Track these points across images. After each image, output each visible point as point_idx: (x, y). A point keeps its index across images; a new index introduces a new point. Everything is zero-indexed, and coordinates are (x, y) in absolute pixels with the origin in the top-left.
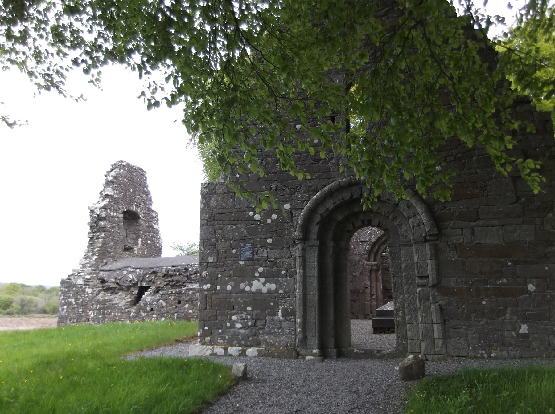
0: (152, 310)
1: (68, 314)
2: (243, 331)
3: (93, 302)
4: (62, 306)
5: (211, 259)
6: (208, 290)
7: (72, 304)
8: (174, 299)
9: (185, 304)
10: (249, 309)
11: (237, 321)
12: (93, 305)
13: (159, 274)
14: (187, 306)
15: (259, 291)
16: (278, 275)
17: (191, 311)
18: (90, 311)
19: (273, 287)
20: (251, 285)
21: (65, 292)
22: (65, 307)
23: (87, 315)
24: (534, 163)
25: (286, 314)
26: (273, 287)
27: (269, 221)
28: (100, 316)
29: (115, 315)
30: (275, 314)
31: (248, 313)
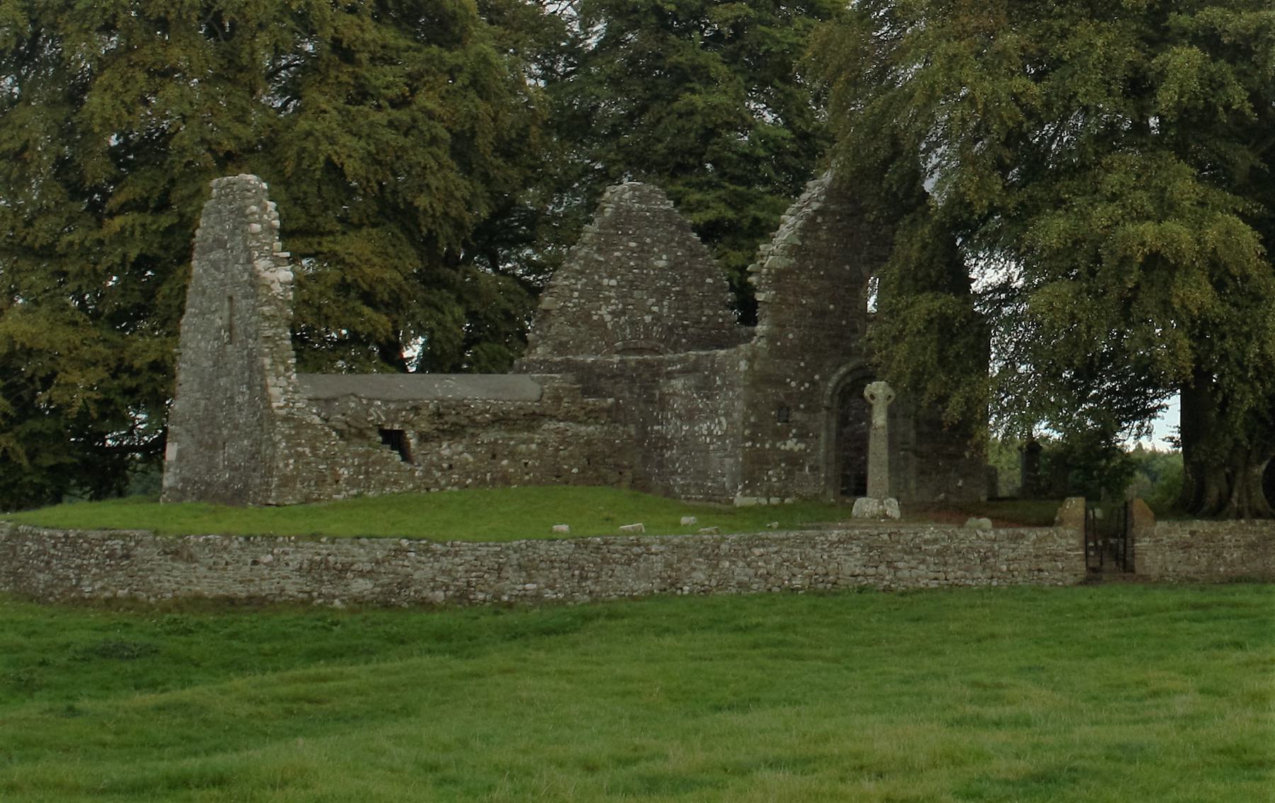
0: (451, 467)
1: (298, 473)
2: (777, 484)
3: (347, 454)
4: (283, 460)
5: (752, 419)
6: (749, 447)
7: (306, 455)
8: (486, 452)
9: (502, 460)
10: (783, 465)
11: (773, 476)
12: (345, 458)
13: (424, 412)
14: (505, 462)
15: (792, 450)
16: (807, 436)
17: (511, 470)
18: (341, 468)
19: (802, 446)
20: (785, 444)
21: (290, 435)
22: (291, 461)
23: (335, 473)
24: (669, 195)
25: (811, 468)
26: (802, 446)
27: (802, 388)
28: (361, 477)
29: (388, 476)
30: (802, 470)
31: (783, 469)
